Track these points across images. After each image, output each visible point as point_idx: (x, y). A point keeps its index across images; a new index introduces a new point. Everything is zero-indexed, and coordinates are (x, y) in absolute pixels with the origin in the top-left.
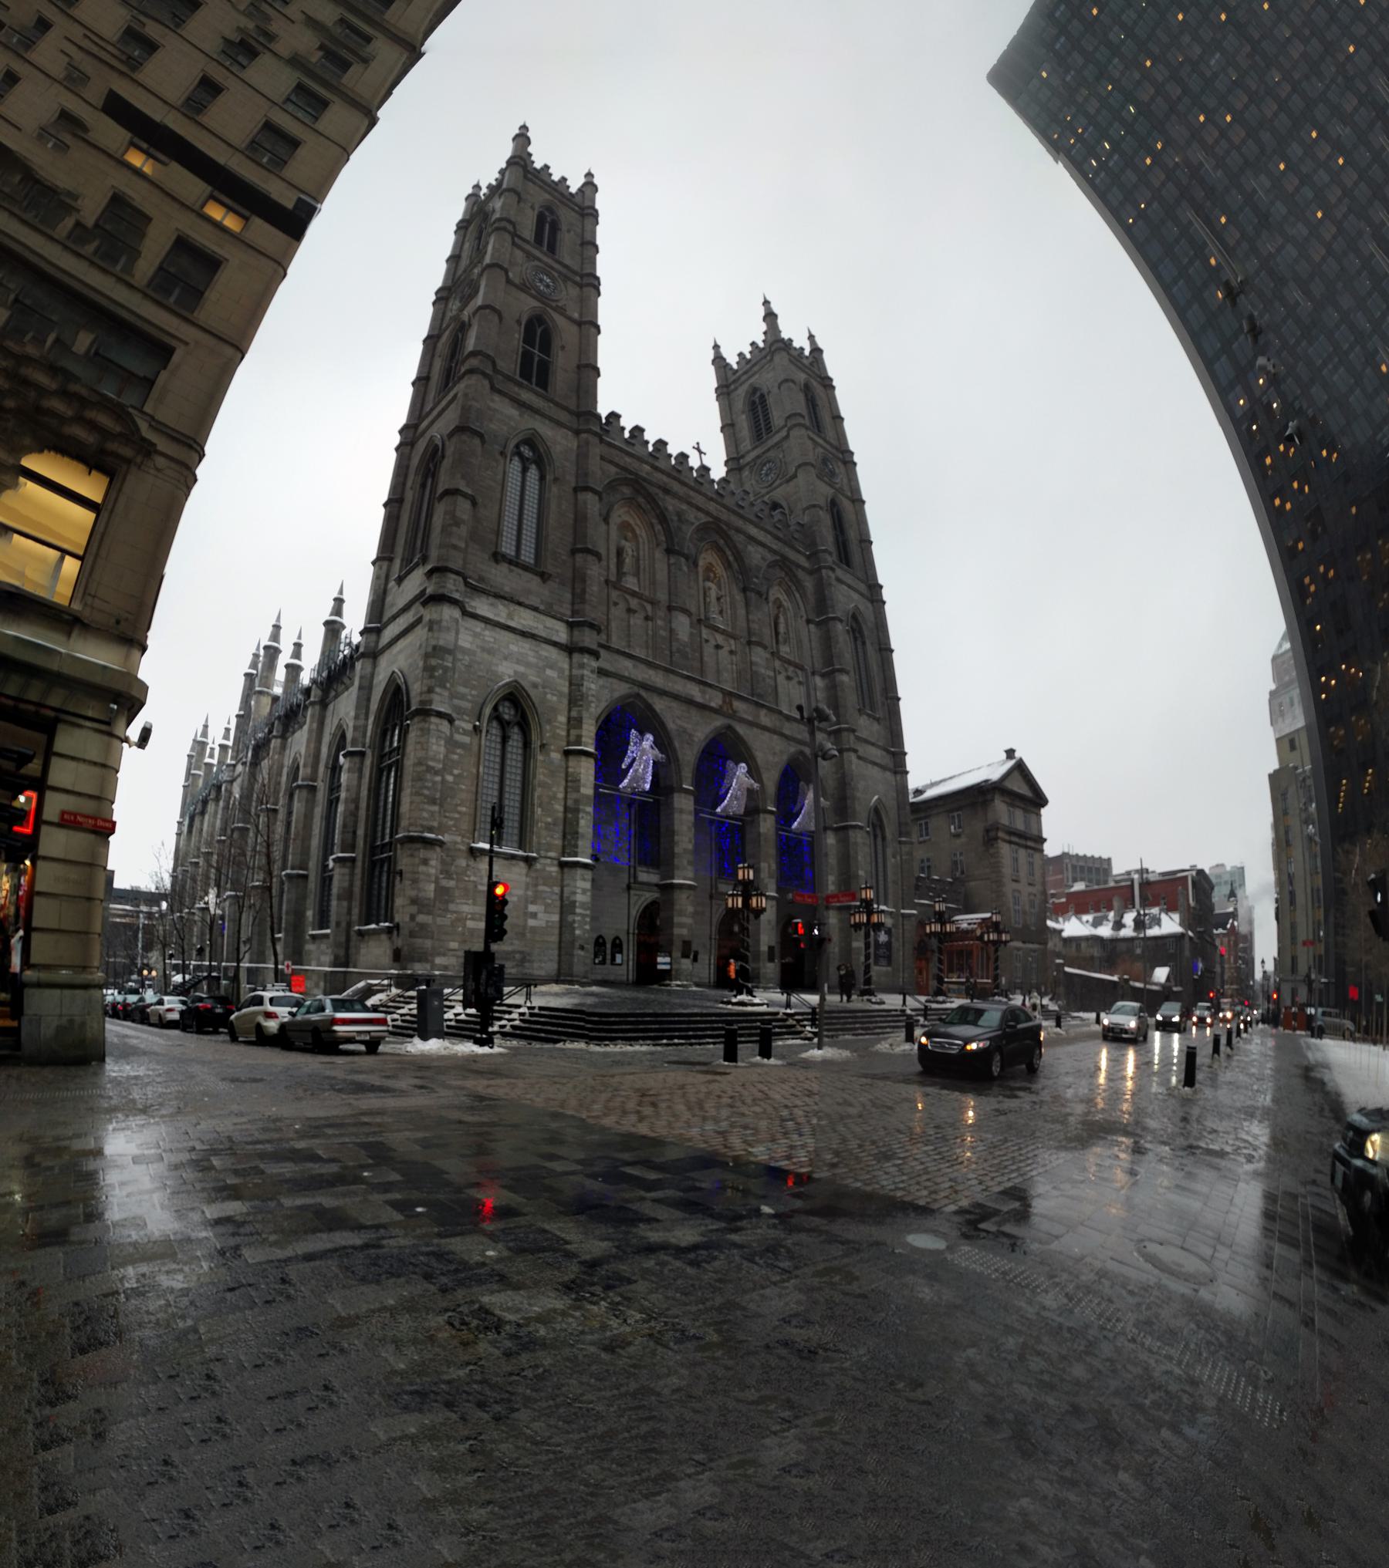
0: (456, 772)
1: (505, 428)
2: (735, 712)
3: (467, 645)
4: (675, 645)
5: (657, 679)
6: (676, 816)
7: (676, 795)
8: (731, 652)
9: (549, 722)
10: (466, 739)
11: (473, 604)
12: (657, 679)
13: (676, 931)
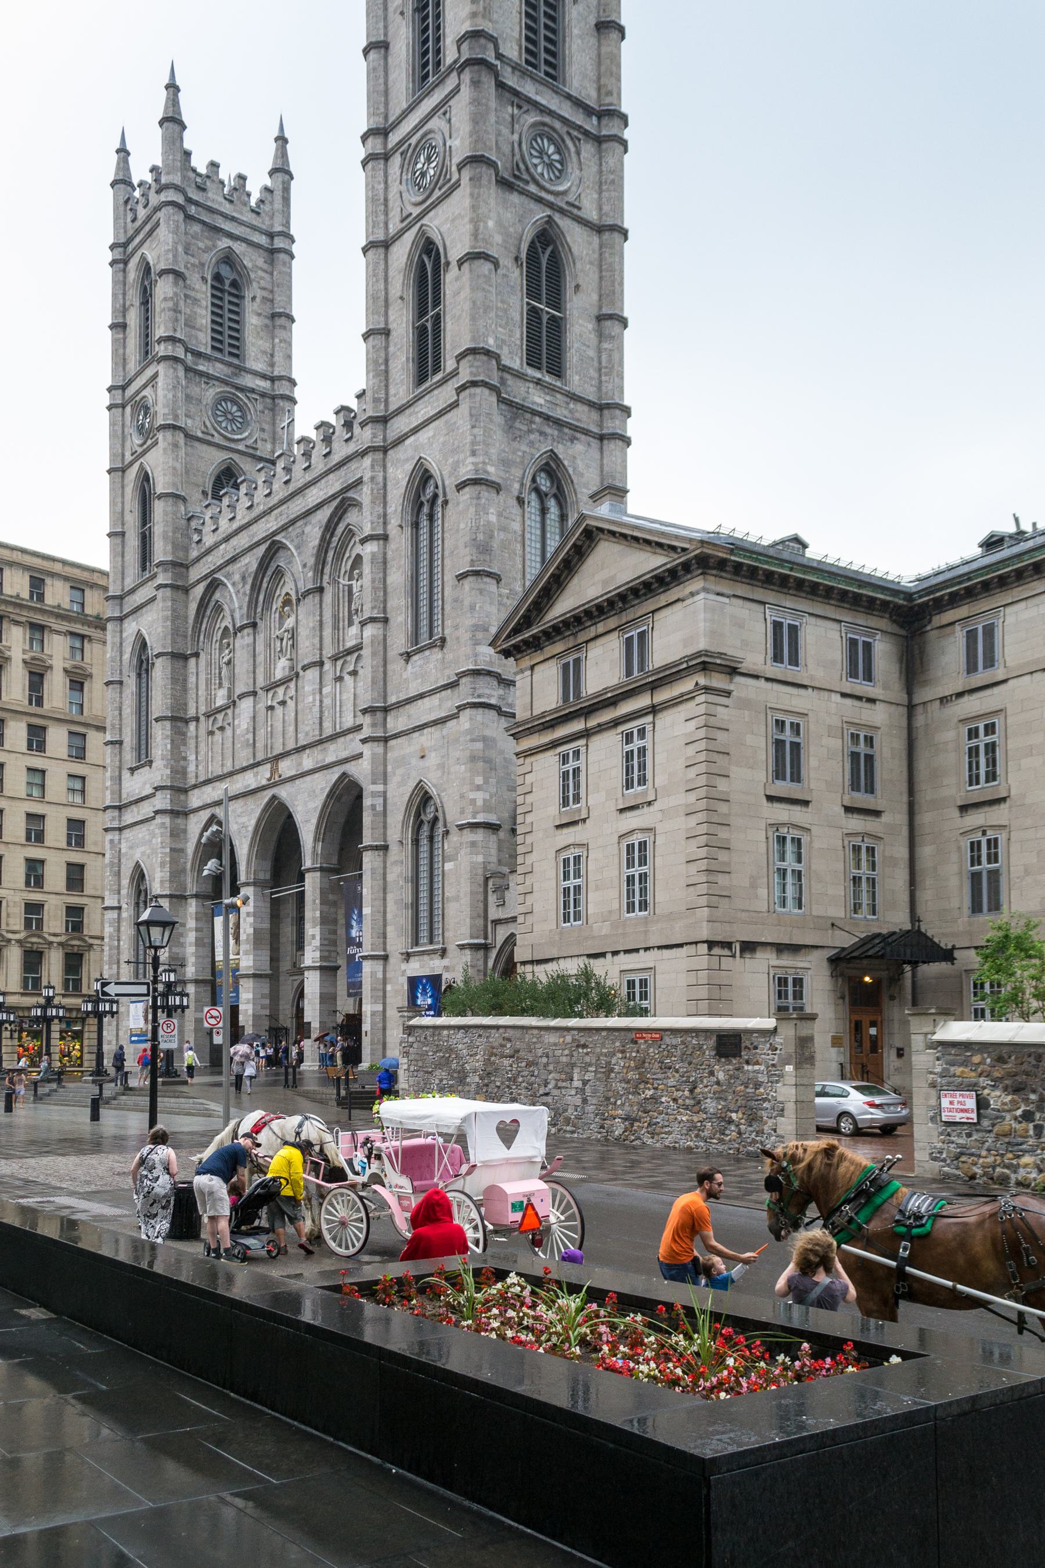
8: (291, 698)
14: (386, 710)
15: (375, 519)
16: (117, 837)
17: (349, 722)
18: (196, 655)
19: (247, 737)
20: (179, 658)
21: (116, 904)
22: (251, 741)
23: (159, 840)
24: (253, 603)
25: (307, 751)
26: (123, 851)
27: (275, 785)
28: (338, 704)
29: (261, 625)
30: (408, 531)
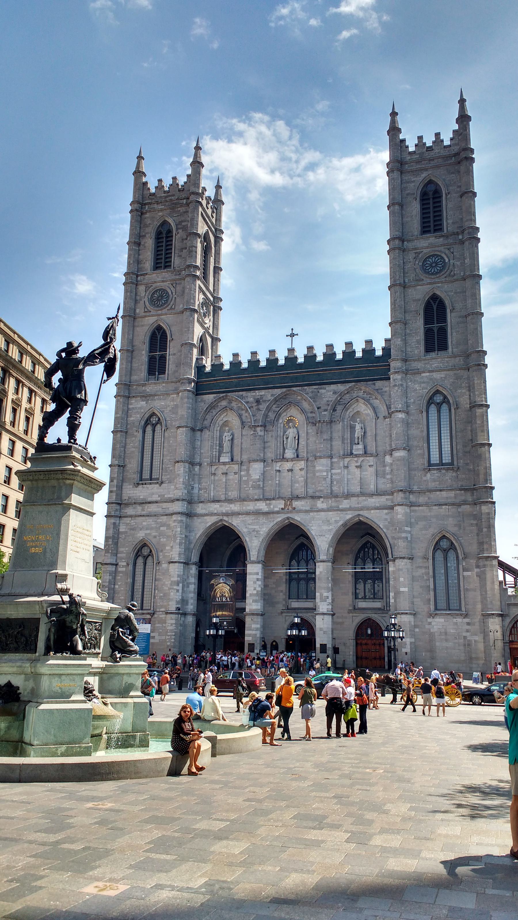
0: (119, 583)
1: (138, 416)
2: (294, 508)
3: (124, 530)
4: (251, 483)
5: (235, 507)
6: (248, 577)
7: (248, 565)
9: (162, 551)
10: (124, 569)
11: (126, 511)
12: (235, 507)
13: (246, 638)
14: (411, 492)
15: (403, 403)
16: (118, 522)
17: (357, 489)
18: (201, 430)
19: (258, 483)
20: (193, 430)
21: (114, 563)
22: (262, 486)
23: (179, 529)
24: (266, 416)
25: (322, 500)
26: (120, 530)
27: (291, 512)
28: (346, 480)
29: (270, 427)
30: (424, 414)
